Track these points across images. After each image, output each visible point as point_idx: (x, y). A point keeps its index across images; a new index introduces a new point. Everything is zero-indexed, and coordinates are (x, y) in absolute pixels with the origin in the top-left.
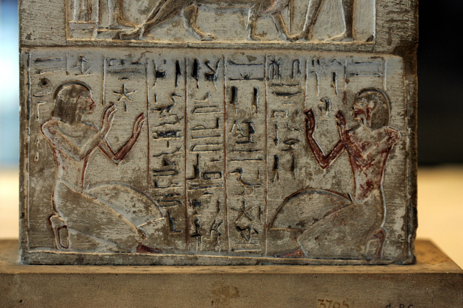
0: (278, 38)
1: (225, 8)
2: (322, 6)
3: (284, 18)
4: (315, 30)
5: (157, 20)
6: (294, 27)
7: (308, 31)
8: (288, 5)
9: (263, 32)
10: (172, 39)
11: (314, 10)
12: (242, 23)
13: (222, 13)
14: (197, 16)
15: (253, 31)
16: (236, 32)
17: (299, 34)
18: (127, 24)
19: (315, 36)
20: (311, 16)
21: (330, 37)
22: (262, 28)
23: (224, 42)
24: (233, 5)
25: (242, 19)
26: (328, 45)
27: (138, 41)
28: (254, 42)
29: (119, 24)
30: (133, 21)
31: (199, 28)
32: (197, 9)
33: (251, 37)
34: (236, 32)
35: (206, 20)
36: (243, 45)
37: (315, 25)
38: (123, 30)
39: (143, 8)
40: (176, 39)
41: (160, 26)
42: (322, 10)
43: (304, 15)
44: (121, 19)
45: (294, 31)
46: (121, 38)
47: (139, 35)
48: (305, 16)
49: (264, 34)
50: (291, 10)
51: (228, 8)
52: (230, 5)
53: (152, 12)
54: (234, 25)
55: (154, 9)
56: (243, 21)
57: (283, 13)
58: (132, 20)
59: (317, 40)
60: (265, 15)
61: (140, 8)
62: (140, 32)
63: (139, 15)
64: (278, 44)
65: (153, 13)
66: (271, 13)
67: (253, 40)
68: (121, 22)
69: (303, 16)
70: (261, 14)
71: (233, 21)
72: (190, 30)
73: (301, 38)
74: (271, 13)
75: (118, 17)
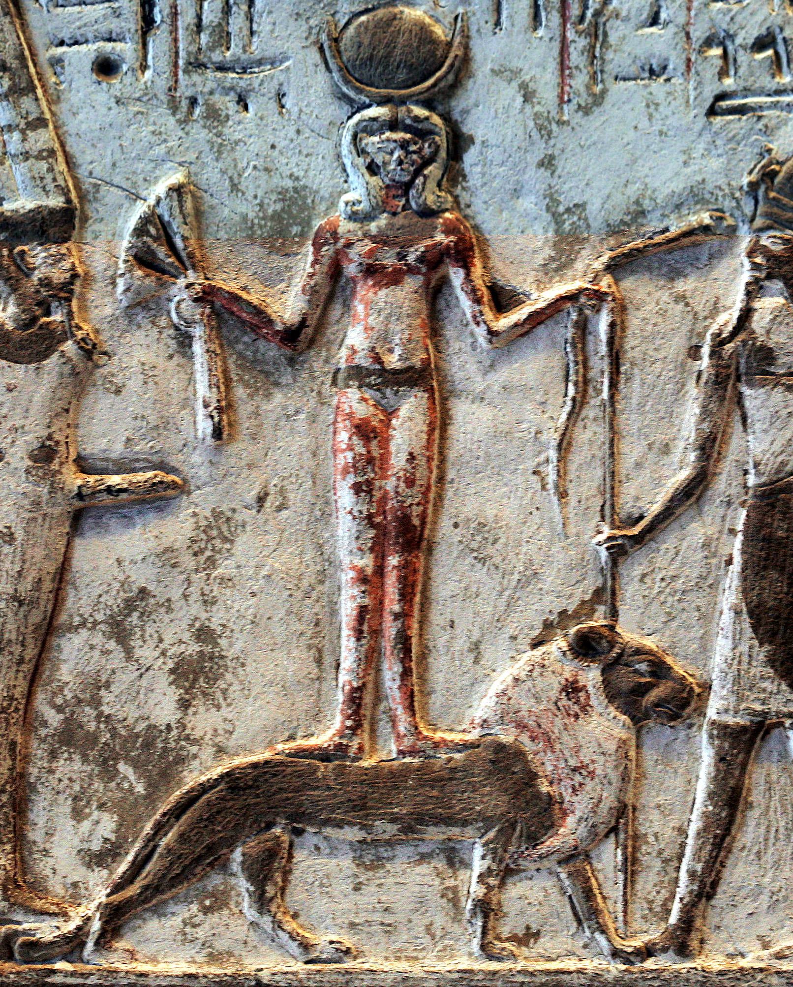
0: (584, 953)
1: (389, 843)
2: (740, 828)
3: (600, 876)
4: (713, 919)
5: (146, 888)
6: (638, 909)
7: (687, 923)
8: (614, 830)
9: (528, 928)
10: (200, 958)
11: (709, 848)
12: (453, 897)
13: (379, 859)
14: (290, 871)
15: (490, 925)
16: (428, 928)
17: (654, 934)
18: (38, 904)
19: (713, 940)
20: (699, 867)
21: (766, 946)
22: (522, 912)
23: (387, 966)
24: (419, 832)
25: (451, 883)
26: (759, 976)
27: (80, 967)
28: (494, 966)
29: (14, 904)
30: (61, 891)
31: (295, 916)
32: (291, 845)
33: (483, 947)
34: (428, 928)
35: (321, 885)
36: (455, 976)
37: (713, 902)
38: (26, 926)
39: (96, 846)
40: (214, 958)
41: (159, 911)
42: (738, 845)
43: (675, 863)
44: (19, 887)
45: (637, 924)
46: (17, 956)
47: (83, 944)
48: (678, 869)
49: (529, 937)
50: (625, 847)
51: (401, 842)
52: (408, 829)
53: (130, 858)
54: (422, 901)
55: (137, 846)
56: (455, 890)
57: (599, 856)
58: (56, 887)
59: (721, 958)
60: (533, 866)
61: (85, 846)
62: (88, 934)
63: (83, 870)
64: (581, 971)
65: (133, 863)
66: (555, 857)
67: (491, 957)
68: (20, 896)
69: (670, 869)
70: (521, 861)
71: (417, 889)
72: (266, 922)
73: (665, 950)
74: (555, 857)
75: (7, 879)
